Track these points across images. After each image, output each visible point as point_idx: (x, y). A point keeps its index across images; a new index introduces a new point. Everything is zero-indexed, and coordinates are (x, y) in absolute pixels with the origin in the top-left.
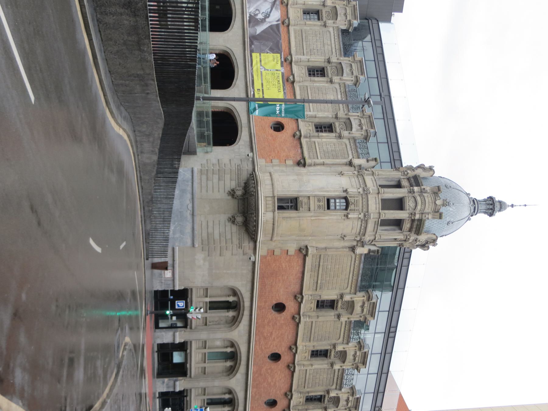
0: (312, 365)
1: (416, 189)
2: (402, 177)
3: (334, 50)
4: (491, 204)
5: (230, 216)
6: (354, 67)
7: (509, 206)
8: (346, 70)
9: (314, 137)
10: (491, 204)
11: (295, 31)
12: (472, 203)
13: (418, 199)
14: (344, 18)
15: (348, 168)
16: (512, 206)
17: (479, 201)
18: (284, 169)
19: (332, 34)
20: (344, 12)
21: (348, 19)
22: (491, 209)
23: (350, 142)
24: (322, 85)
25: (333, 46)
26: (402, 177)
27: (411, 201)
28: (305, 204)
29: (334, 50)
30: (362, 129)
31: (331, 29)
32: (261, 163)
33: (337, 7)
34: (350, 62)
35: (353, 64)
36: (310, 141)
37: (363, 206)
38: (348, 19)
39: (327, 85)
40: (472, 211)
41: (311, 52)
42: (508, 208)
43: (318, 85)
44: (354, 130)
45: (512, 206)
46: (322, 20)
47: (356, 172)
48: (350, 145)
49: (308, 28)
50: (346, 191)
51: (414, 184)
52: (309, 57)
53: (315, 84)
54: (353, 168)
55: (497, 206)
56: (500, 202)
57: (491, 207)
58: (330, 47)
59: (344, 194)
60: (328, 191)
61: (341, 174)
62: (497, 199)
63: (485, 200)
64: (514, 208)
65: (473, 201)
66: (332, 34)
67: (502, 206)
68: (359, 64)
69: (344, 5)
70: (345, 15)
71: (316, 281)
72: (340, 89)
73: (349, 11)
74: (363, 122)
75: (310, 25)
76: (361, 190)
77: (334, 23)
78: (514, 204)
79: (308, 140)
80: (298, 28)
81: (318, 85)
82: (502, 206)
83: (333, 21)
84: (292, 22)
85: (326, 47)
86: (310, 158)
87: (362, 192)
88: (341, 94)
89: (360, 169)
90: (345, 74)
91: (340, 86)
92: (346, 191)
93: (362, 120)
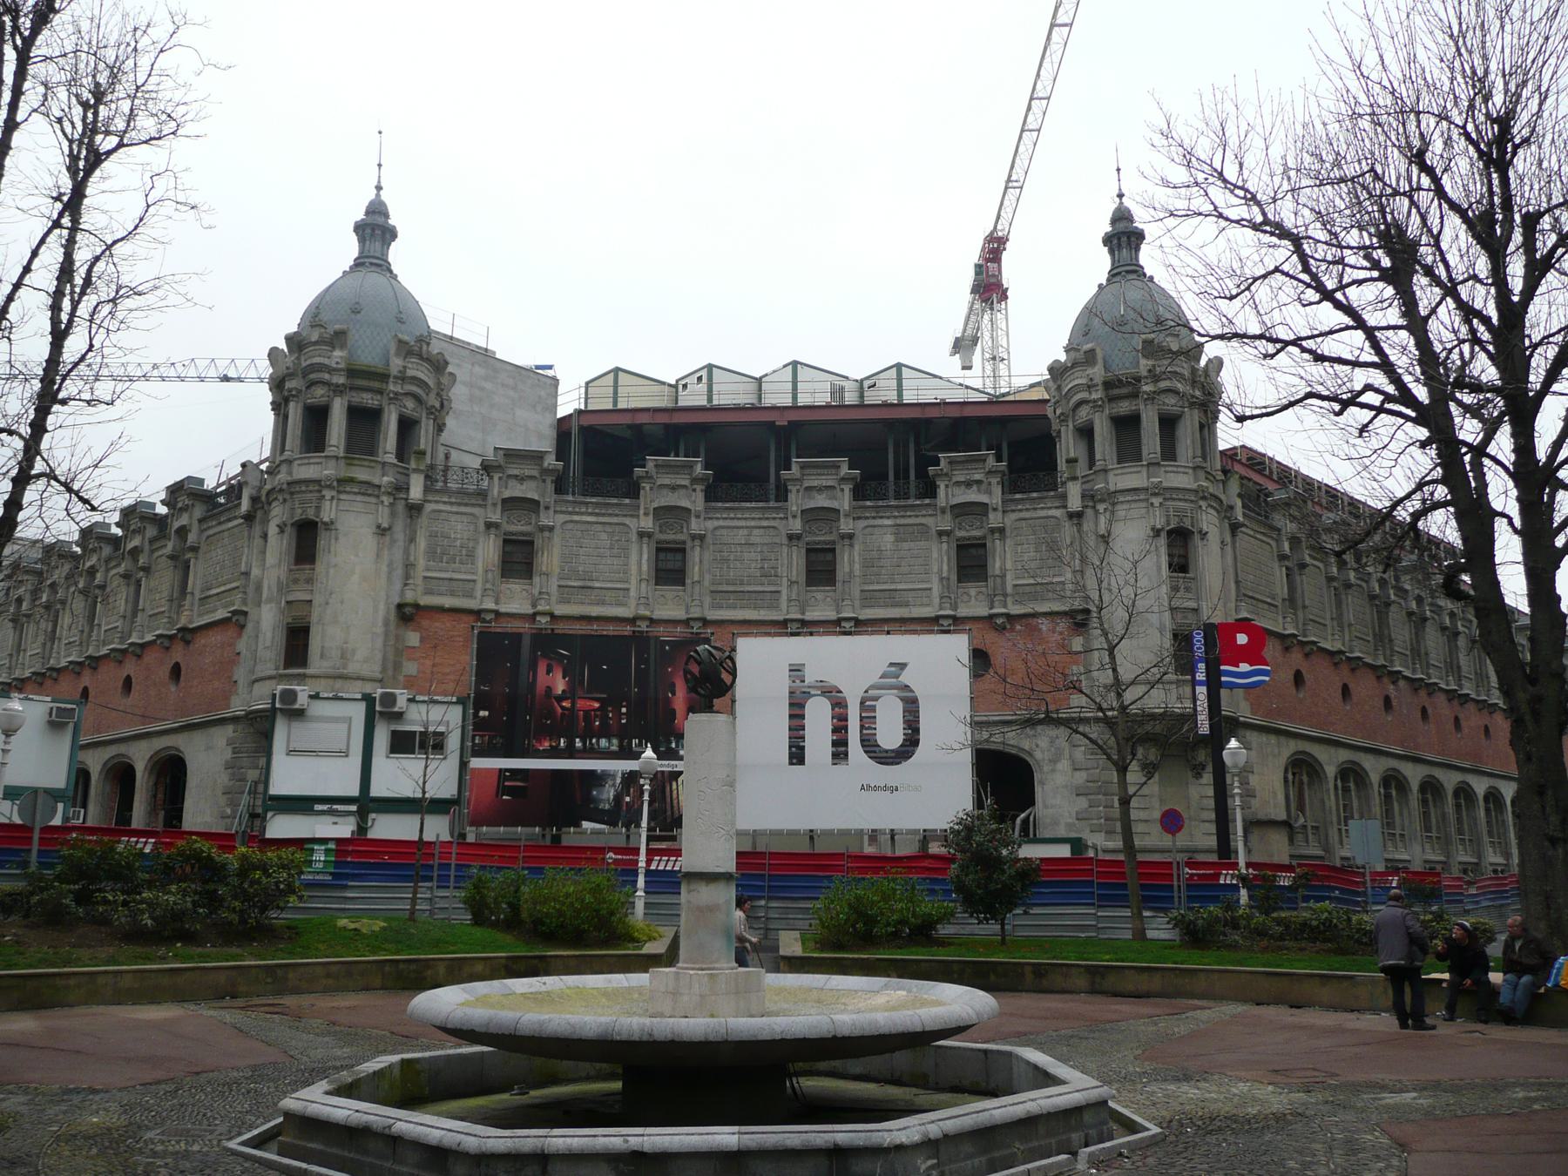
0: (1350, 625)
1: (1147, 388)
2: (1107, 411)
3: (765, 523)
4: (1119, 239)
5: (1190, 774)
6: (815, 483)
7: (1121, 203)
8: (821, 501)
9: (1004, 583)
10: (1119, 239)
11: (714, 606)
12: (1117, 279)
13: (1163, 384)
14: (683, 492)
15: (1087, 525)
17: (1113, 264)
19: (721, 523)
20: (665, 491)
21: (686, 483)
22: (1129, 238)
23: (1013, 511)
24: (857, 559)
25: (753, 523)
26: (1107, 411)
27: (1167, 401)
28: (1186, 618)
29: (765, 523)
30: (979, 482)
31: (710, 524)
33: (655, 505)
34: (802, 490)
35: (806, 484)
36: (1013, 595)
37: (1186, 500)
38: (686, 483)
39: (857, 547)
40: (1134, 276)
41: (770, 575)
43: (857, 566)
44: (984, 498)
45: (1121, 196)
46: (684, 542)
47: (1101, 507)
48: (1020, 510)
49: (707, 577)
50: (1157, 533)
52: (785, 579)
53: (857, 573)
54: (1089, 512)
55: (1121, 226)
56: (1114, 221)
57: (1124, 239)
58: (756, 532)
59: (1164, 534)
60: (1159, 568)
61: (1105, 539)
62: (1109, 229)
63: (1111, 252)
64: (1124, 191)
65: (1114, 276)
66: (721, 523)
68: (807, 471)
69: (651, 489)
70: (674, 488)
71: (1266, 606)
72: (867, 518)
73: (666, 480)
74: (962, 479)
75: (701, 574)
76: (1156, 501)
77: (698, 517)
78: (1117, 192)
79: (1009, 600)
80: (707, 600)
81: (857, 566)
83: (693, 519)
84: (695, 613)
85: (753, 540)
87: (1160, 500)
88: (881, 517)
89: (1093, 497)
90: (835, 505)
91: (859, 518)
92: (1157, 533)
93: (954, 479)
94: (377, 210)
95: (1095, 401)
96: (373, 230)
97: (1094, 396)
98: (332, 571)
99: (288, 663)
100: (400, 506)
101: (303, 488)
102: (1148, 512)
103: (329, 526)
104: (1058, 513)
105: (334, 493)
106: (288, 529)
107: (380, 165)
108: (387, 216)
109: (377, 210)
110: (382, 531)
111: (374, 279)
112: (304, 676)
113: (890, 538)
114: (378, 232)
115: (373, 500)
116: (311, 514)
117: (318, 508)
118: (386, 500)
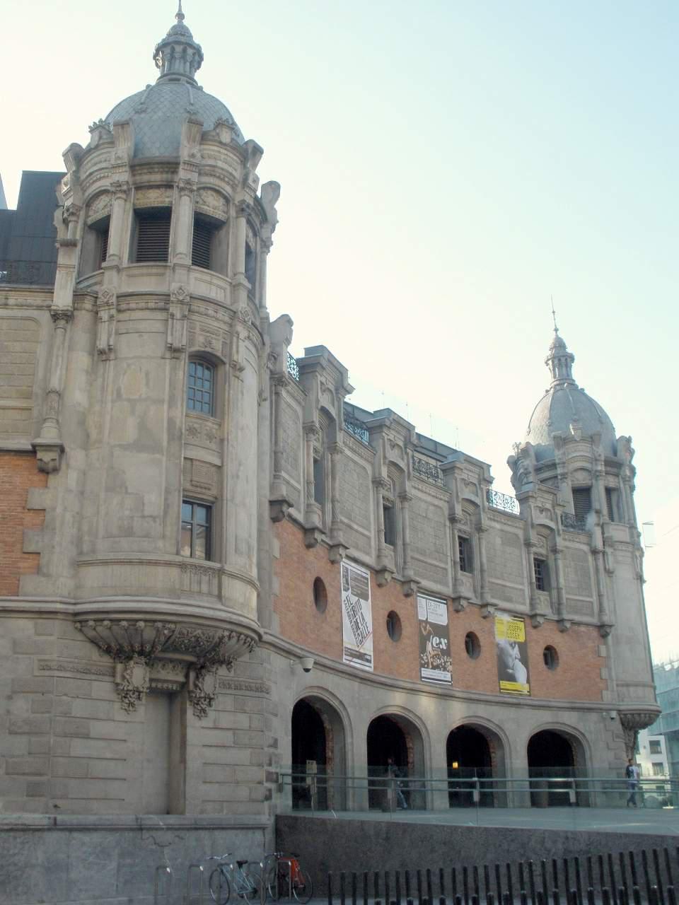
7: (557, 336)
10: (559, 360)
16: (556, 330)
18: (612, 660)
32: (608, 696)
42: (560, 336)
44: (552, 525)
45: (556, 330)
51: (615, 470)
67: (559, 345)
82: (559, 345)
86: (592, 615)
88: (494, 520)
95: (600, 472)
96: (184, 51)
97: (599, 468)
98: (240, 433)
101: (211, 312)
102: (633, 561)
104: (586, 548)
113: (498, 541)
116: (217, 348)
117: (228, 345)
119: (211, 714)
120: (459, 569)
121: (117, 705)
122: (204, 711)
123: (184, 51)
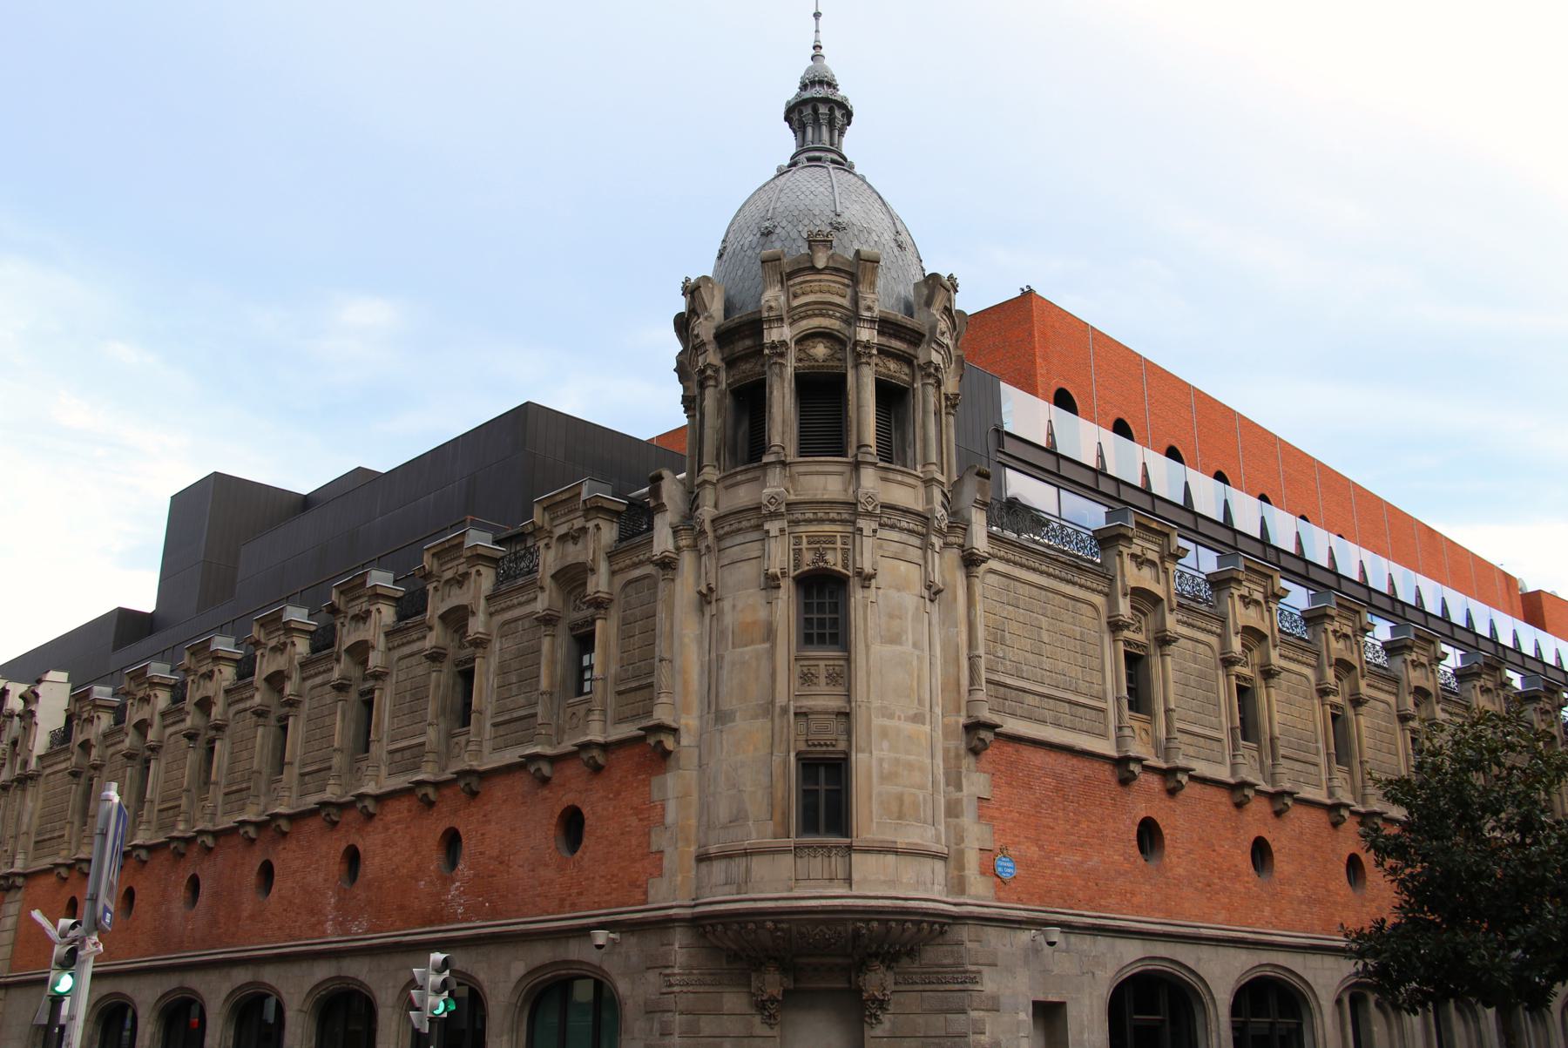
94: (817, 80)
99: (809, 823)
100: (953, 555)
103: (866, 579)
105: (874, 525)
106: (787, 585)
107: (817, 15)
108: (831, 85)
109: (817, 80)
110: (934, 592)
111: (813, 185)
112: (850, 849)
114: (823, 110)
115: (916, 541)
116: (834, 561)
118: (937, 541)
119: (886, 1019)
120: (1335, 762)
121: (757, 1019)
122: (876, 1017)
123: (815, 111)
